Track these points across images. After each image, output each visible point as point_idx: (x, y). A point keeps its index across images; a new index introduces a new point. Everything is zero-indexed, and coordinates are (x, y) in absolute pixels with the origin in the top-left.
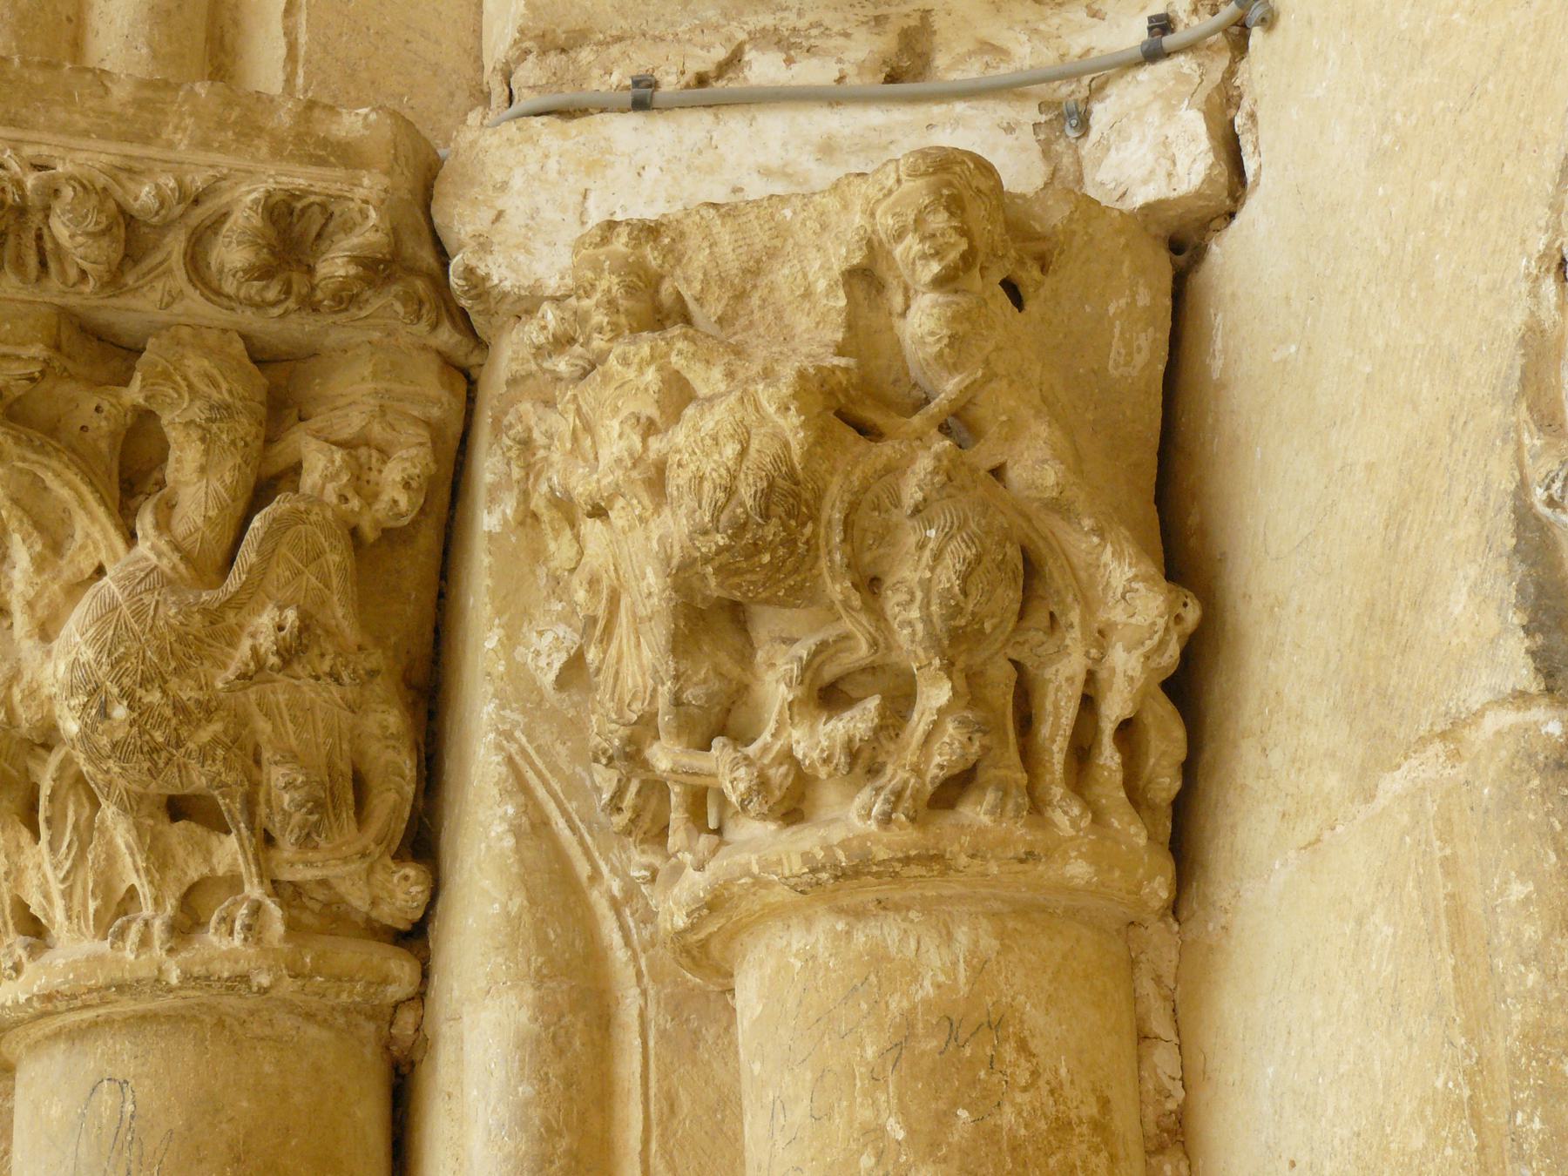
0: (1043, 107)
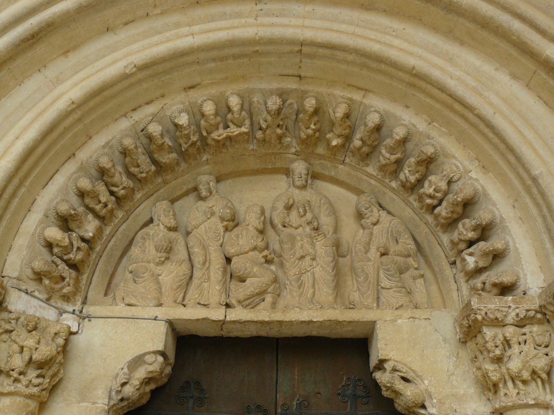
0: (59, 311)
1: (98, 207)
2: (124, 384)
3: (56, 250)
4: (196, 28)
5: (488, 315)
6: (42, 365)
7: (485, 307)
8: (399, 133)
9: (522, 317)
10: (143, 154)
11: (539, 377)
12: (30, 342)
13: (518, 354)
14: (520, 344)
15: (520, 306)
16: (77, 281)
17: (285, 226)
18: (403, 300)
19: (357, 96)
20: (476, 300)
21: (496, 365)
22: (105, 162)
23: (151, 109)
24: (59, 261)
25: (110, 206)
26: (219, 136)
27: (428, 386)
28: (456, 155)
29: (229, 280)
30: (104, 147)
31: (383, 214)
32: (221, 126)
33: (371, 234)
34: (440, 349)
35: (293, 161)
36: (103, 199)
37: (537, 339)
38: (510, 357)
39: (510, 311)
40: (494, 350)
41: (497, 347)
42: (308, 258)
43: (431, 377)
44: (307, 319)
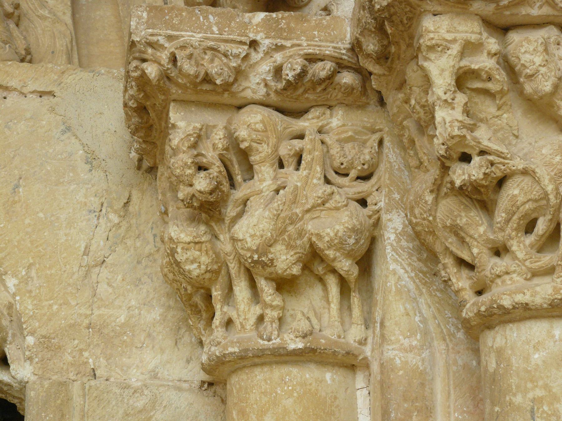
5: (179, 64)
7: (170, 38)
9: (290, 77)
11: (334, 271)
13: (268, 193)
14: (281, 165)
15: (288, 44)
20: (145, 15)
21: (203, 228)
27: (14, 295)
34: (73, 187)
37: (335, 150)
38: (245, 204)
39: (255, 57)
40: (192, 176)
41: (201, 168)
43: (30, 266)
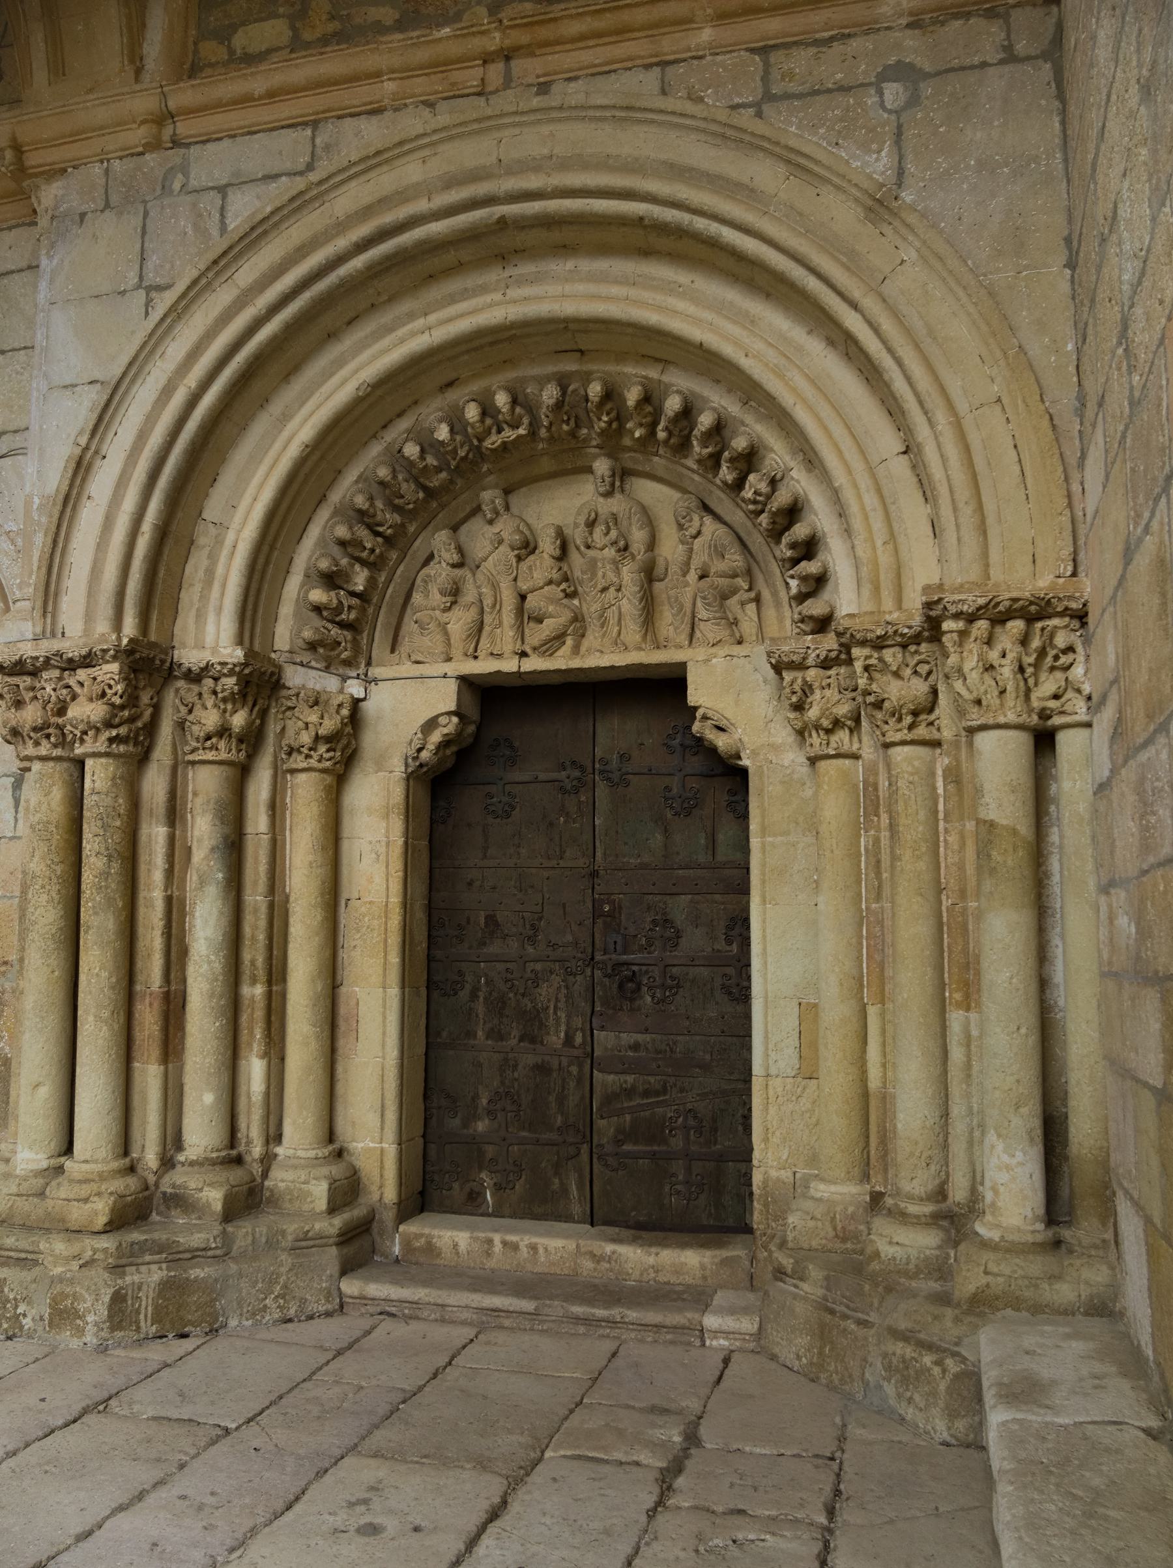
1: (364, 554)
2: (420, 750)
3: (325, 613)
4: (432, 318)
6: (331, 739)
8: (705, 421)
10: (407, 481)
12: (313, 718)
16: (355, 643)
17: (588, 547)
18: (724, 633)
19: (653, 373)
22: (360, 501)
23: (404, 424)
24: (330, 626)
25: (378, 551)
26: (493, 444)
28: (775, 448)
29: (526, 620)
30: (357, 482)
31: (708, 520)
32: (494, 430)
33: (691, 550)
35: (595, 457)
36: (368, 545)
41: (794, 693)
42: (612, 589)
44: (608, 664)
